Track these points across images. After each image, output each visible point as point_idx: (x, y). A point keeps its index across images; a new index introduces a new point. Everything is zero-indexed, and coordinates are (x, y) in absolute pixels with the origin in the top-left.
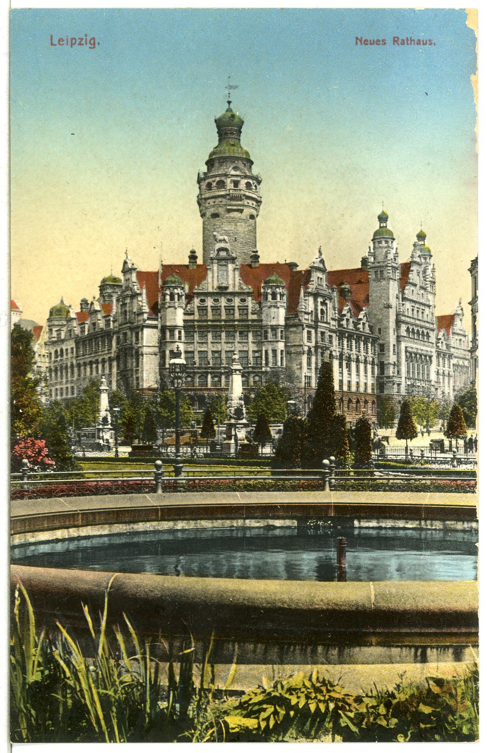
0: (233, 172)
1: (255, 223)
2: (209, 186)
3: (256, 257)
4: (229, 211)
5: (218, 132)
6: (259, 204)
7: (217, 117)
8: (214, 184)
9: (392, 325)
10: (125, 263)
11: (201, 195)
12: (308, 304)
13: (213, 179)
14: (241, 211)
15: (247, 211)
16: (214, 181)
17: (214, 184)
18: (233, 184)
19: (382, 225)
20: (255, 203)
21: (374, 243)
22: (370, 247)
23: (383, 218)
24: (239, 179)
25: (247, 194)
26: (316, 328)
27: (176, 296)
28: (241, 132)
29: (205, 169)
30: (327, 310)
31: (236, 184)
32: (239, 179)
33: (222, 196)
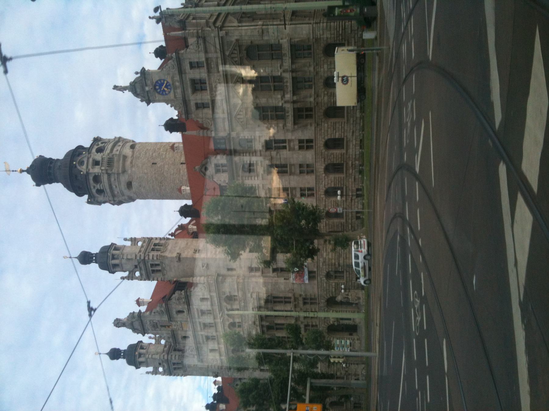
1: (140, 143)
2: (100, 192)
4: (124, 171)
6: (121, 140)
7: (35, 184)
8: (98, 187)
11: (110, 201)
13: (92, 187)
14: (125, 157)
15: (127, 151)
16: (94, 187)
17: (98, 187)
18: (97, 167)
24: (91, 160)
25: (108, 151)
28: (51, 159)
29: (86, 197)
31: (96, 163)
32: (91, 160)
33: (109, 180)
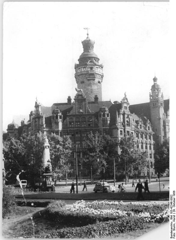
0: (90, 64)
3: (96, 98)
5: (83, 47)
7: (83, 41)
9: (162, 127)
10: (36, 103)
12: (120, 119)
19: (155, 83)
20: (100, 76)
21: (152, 91)
22: (150, 93)
23: (155, 80)
24: (92, 66)
26: (124, 129)
27: (59, 117)
29: (78, 63)
30: (129, 121)
32: (92, 66)
